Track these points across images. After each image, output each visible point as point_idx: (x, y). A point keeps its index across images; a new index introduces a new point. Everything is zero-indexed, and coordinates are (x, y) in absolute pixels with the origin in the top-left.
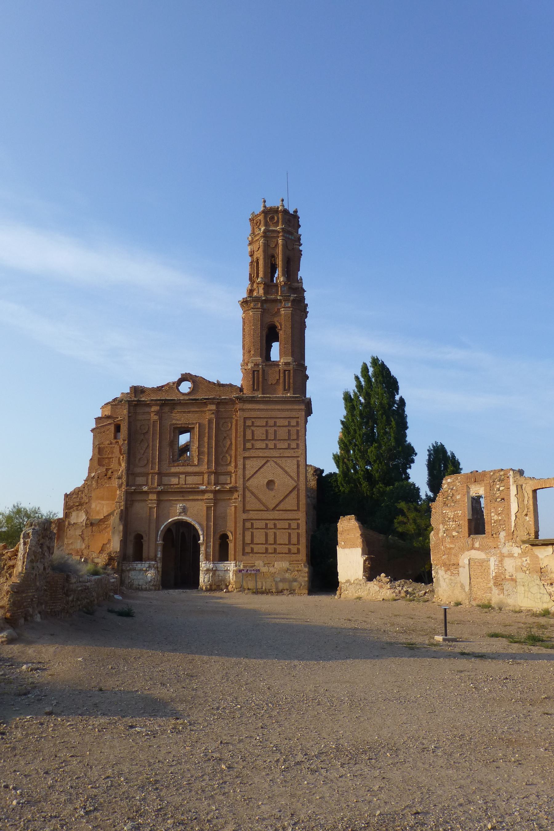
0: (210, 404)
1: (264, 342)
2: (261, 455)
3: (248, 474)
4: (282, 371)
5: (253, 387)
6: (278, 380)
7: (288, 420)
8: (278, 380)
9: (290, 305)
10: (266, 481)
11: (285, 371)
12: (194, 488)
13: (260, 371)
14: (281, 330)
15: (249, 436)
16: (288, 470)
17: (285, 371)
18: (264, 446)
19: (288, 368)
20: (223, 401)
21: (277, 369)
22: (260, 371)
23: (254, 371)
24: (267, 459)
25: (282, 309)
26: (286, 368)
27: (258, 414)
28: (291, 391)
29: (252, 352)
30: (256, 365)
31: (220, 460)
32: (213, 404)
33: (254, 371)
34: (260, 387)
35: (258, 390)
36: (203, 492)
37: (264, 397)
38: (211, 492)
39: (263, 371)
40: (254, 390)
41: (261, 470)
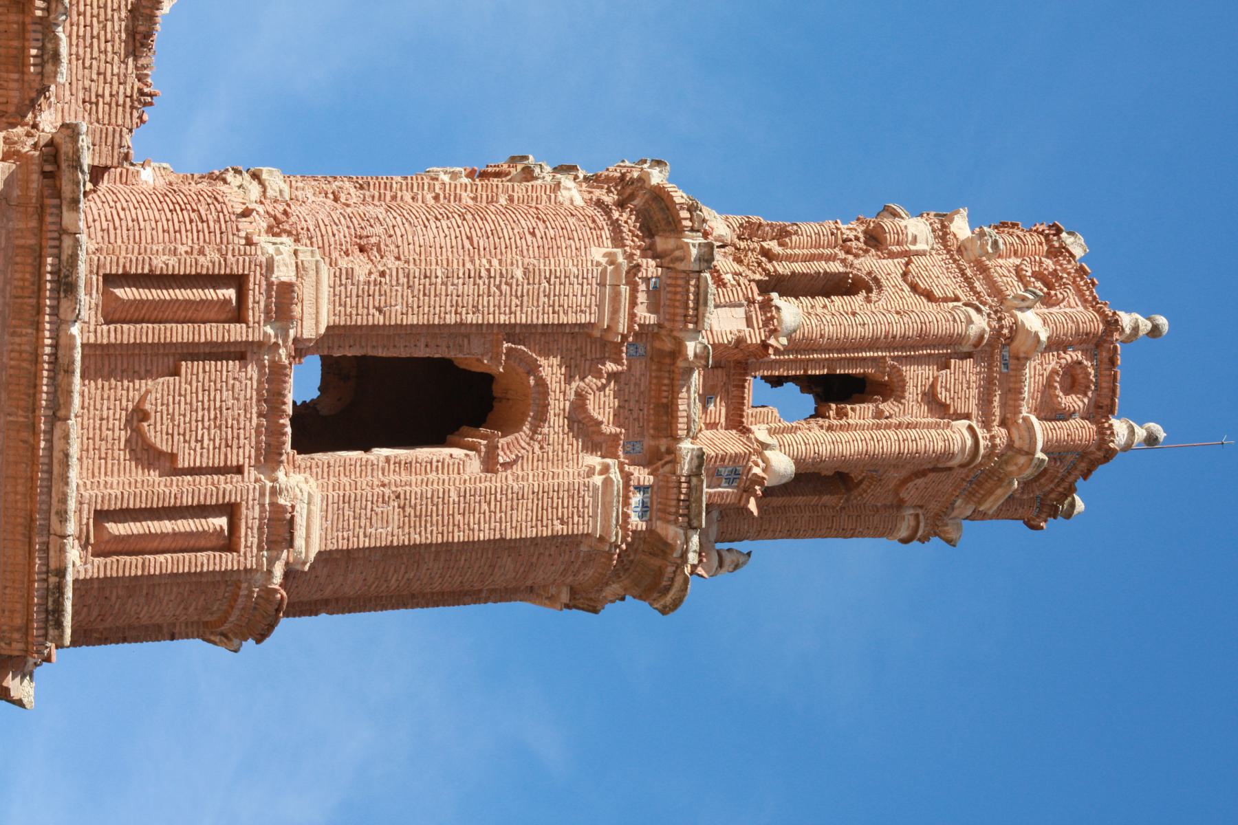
1: (421, 352)
4: (229, 487)
5: (127, 279)
6: (165, 463)
8: (165, 463)
9: (636, 522)
11: (231, 510)
13: (237, 332)
14: (490, 464)
17: (231, 510)
19: (249, 537)
21: (244, 454)
22: (237, 332)
23: (239, 282)
25: (615, 475)
26: (251, 517)
28: (96, 567)
29: (361, 267)
30: (283, 301)
33: (239, 282)
34: (129, 333)
35: (113, 314)
37: (60, 368)
39: (239, 353)
40: (111, 280)
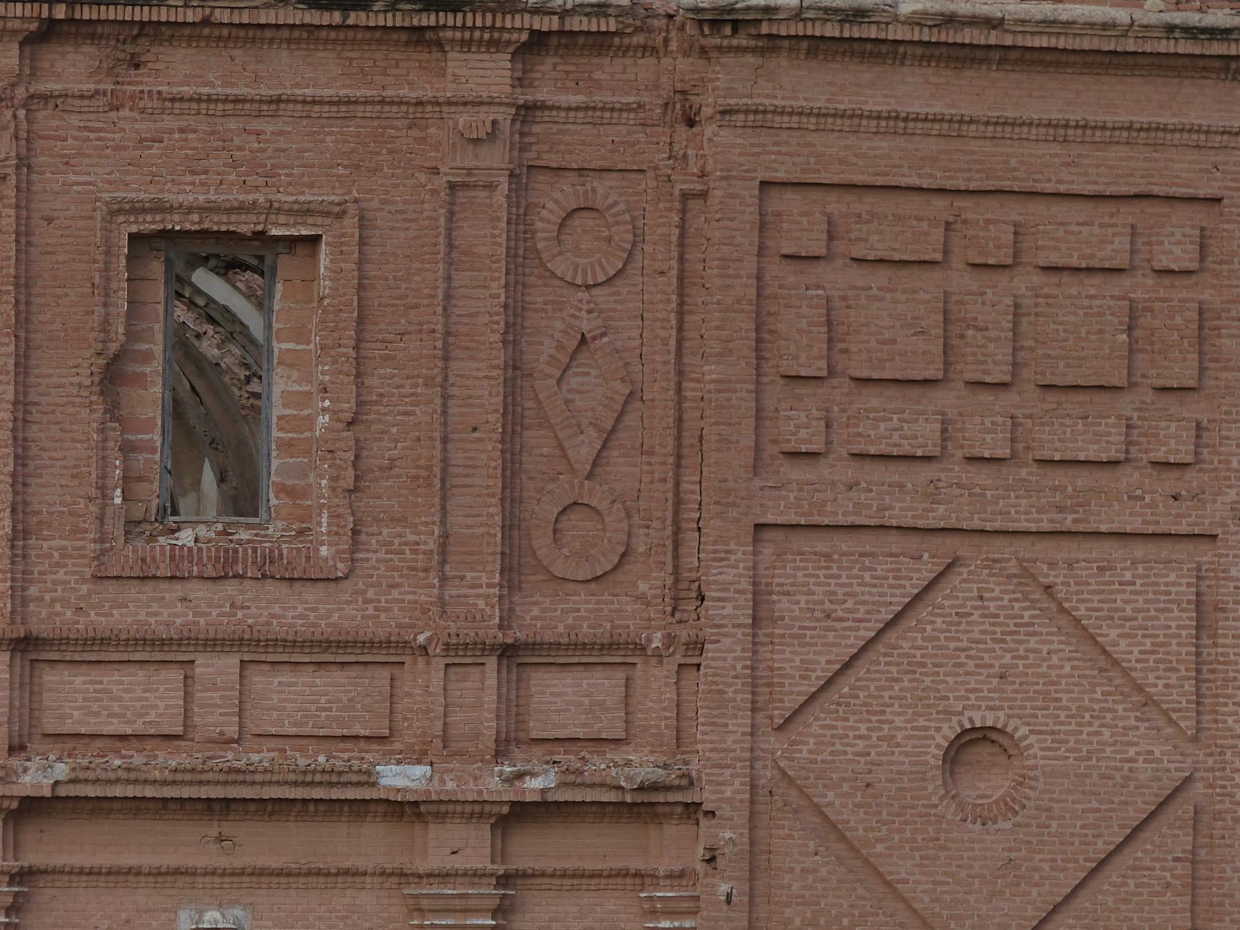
0: (466, 45)
2: (902, 512)
3: (797, 666)
7: (1129, 213)
10: (949, 731)
12: (332, 777)
15: (801, 350)
16: (1128, 651)
18: (925, 435)
20: (576, 24)
24: (951, 544)
27: (878, 156)
31: (542, 542)
32: (494, 45)
36: (406, 811)
38: (475, 811)
41: (904, 641)
